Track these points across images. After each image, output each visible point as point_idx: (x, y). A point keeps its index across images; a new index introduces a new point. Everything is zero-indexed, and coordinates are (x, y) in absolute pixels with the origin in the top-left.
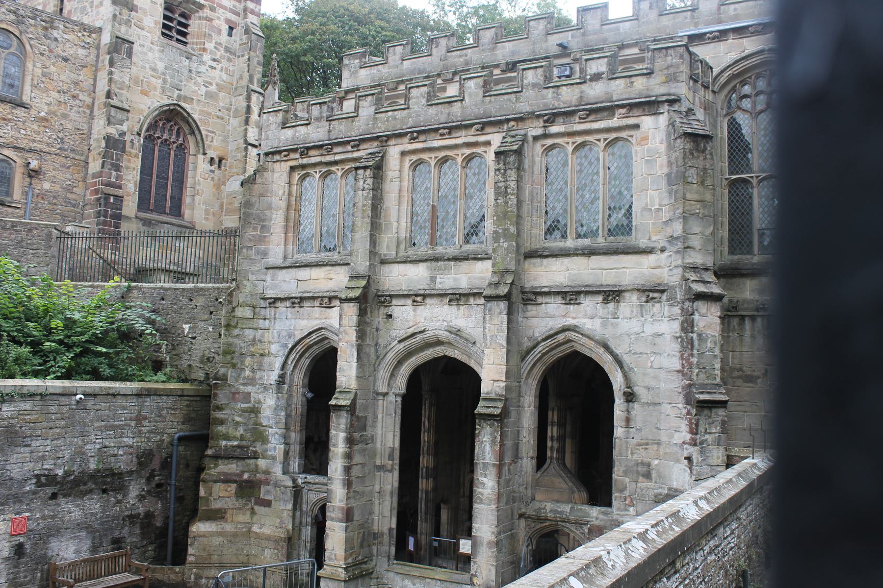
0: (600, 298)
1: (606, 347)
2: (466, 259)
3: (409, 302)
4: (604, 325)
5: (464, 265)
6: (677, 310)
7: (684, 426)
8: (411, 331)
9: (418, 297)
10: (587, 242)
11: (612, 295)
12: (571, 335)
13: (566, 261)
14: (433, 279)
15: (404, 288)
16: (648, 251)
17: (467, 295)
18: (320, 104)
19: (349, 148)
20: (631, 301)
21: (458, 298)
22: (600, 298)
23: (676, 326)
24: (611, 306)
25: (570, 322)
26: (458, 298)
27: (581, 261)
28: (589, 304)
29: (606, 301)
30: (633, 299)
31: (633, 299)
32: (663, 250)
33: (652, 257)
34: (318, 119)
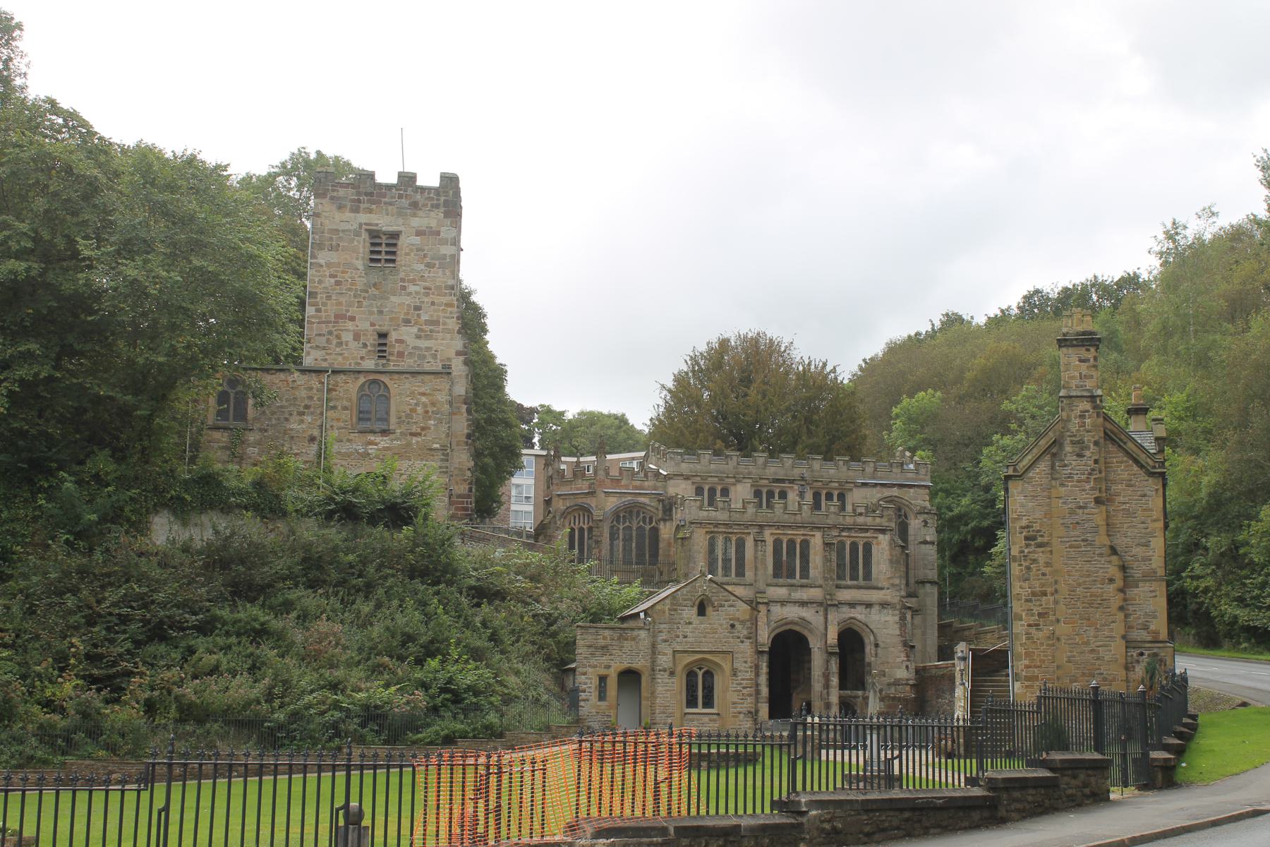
0: (864, 606)
1: (867, 626)
2: (806, 586)
3: (779, 604)
4: (866, 617)
5: (805, 589)
6: (898, 612)
7: (903, 655)
8: (780, 618)
9: (783, 603)
10: (855, 582)
11: (869, 605)
12: (852, 620)
13: (849, 590)
14: (790, 595)
15: (776, 598)
16: (882, 589)
17: (807, 603)
18: (724, 501)
19: (742, 527)
20: (876, 609)
21: (803, 604)
22: (864, 606)
23: (897, 618)
24: (868, 610)
25: (852, 615)
26: (803, 604)
27: (856, 590)
28: (859, 608)
29: (866, 608)
30: (877, 608)
31: (877, 608)
32: (888, 589)
33: (884, 591)
34: (722, 509)
